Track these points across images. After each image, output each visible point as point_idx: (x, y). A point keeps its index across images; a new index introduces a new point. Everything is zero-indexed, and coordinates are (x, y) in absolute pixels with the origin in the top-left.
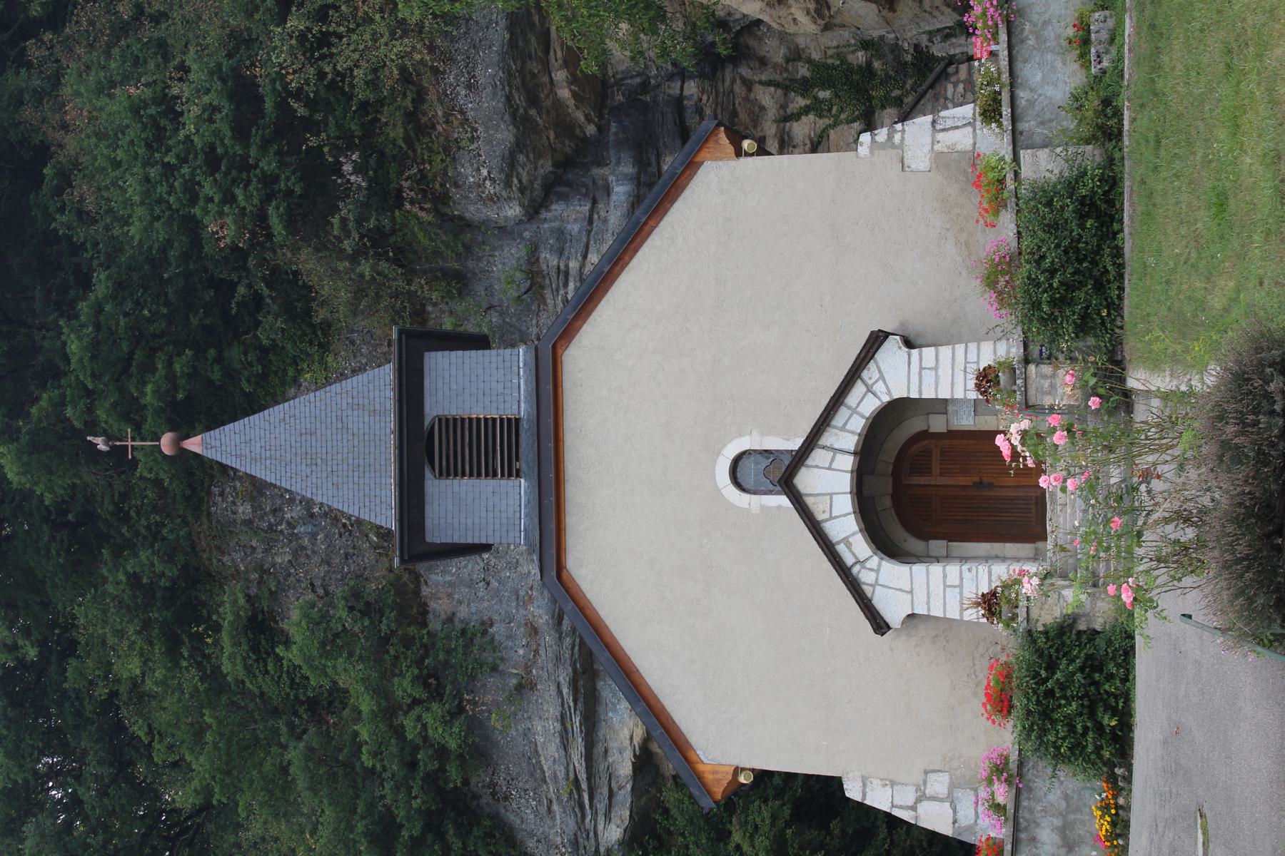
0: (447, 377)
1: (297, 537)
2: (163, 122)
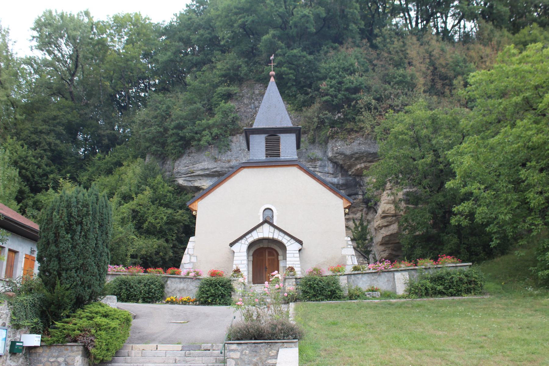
1: (251, 104)
2: (349, 71)
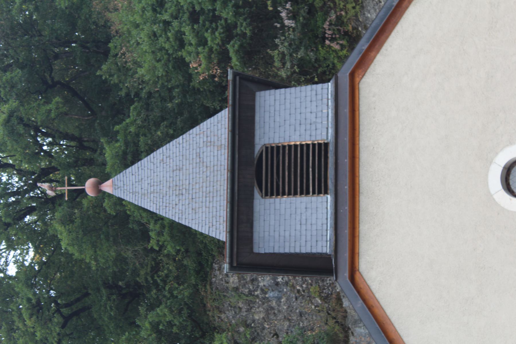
0: (272, 111)
1: (268, 300)
